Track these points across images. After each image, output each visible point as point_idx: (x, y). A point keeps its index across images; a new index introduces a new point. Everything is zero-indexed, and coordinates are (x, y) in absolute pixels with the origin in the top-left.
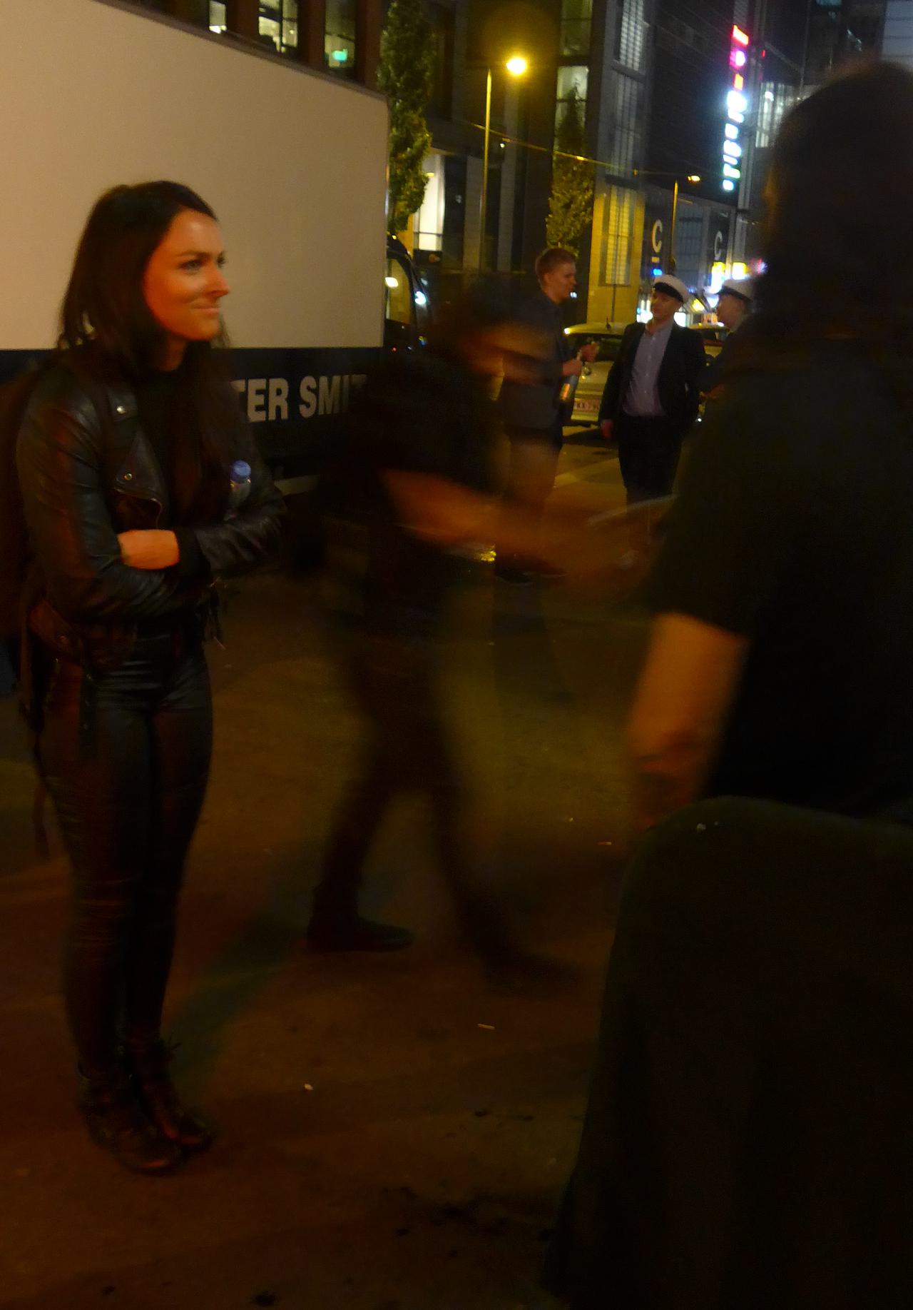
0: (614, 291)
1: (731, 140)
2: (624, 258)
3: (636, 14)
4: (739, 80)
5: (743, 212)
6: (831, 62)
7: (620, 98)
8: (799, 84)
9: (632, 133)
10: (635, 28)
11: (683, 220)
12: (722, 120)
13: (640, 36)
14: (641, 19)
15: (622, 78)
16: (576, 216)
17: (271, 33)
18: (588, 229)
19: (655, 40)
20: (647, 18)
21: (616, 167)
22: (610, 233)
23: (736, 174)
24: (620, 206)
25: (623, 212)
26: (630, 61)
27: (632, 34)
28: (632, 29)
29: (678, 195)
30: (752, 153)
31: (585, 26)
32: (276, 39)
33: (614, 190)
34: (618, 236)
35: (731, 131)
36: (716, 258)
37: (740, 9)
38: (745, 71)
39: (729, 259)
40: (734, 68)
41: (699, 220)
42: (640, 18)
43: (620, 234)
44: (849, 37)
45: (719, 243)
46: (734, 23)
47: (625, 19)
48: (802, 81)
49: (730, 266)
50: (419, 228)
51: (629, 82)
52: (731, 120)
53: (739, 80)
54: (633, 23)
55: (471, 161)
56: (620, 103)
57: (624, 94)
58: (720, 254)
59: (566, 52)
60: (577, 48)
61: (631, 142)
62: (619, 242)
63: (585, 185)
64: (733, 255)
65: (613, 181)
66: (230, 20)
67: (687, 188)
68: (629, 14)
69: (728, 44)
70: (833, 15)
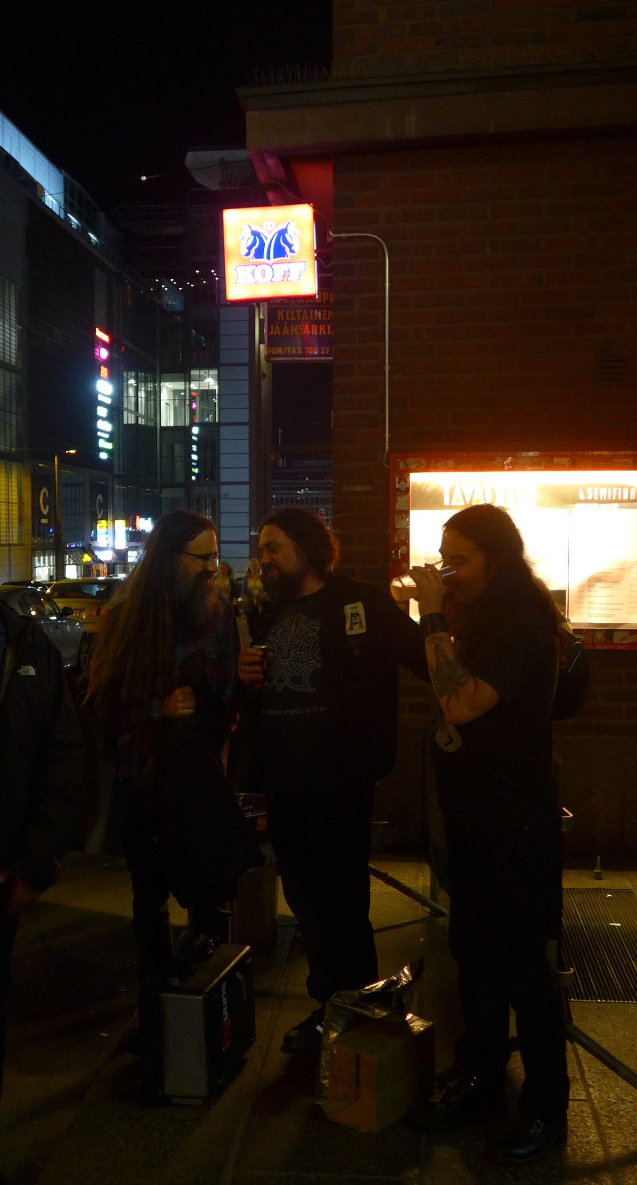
0: (10, 550)
1: (104, 419)
2: (16, 521)
3: (10, 319)
4: (104, 371)
5: (118, 476)
9: (14, 417)
10: (10, 330)
11: (67, 485)
13: (15, 337)
14: (14, 323)
20: (19, 321)
23: (109, 446)
26: (7, 357)
27: (8, 335)
28: (7, 331)
34: (9, 503)
35: (102, 411)
37: (100, 312)
38: (108, 363)
39: (110, 517)
40: (99, 361)
41: (82, 485)
43: (10, 501)
45: (99, 503)
48: (158, 369)
49: (112, 522)
53: (104, 371)
54: (7, 326)
61: (14, 423)
67: (66, 460)
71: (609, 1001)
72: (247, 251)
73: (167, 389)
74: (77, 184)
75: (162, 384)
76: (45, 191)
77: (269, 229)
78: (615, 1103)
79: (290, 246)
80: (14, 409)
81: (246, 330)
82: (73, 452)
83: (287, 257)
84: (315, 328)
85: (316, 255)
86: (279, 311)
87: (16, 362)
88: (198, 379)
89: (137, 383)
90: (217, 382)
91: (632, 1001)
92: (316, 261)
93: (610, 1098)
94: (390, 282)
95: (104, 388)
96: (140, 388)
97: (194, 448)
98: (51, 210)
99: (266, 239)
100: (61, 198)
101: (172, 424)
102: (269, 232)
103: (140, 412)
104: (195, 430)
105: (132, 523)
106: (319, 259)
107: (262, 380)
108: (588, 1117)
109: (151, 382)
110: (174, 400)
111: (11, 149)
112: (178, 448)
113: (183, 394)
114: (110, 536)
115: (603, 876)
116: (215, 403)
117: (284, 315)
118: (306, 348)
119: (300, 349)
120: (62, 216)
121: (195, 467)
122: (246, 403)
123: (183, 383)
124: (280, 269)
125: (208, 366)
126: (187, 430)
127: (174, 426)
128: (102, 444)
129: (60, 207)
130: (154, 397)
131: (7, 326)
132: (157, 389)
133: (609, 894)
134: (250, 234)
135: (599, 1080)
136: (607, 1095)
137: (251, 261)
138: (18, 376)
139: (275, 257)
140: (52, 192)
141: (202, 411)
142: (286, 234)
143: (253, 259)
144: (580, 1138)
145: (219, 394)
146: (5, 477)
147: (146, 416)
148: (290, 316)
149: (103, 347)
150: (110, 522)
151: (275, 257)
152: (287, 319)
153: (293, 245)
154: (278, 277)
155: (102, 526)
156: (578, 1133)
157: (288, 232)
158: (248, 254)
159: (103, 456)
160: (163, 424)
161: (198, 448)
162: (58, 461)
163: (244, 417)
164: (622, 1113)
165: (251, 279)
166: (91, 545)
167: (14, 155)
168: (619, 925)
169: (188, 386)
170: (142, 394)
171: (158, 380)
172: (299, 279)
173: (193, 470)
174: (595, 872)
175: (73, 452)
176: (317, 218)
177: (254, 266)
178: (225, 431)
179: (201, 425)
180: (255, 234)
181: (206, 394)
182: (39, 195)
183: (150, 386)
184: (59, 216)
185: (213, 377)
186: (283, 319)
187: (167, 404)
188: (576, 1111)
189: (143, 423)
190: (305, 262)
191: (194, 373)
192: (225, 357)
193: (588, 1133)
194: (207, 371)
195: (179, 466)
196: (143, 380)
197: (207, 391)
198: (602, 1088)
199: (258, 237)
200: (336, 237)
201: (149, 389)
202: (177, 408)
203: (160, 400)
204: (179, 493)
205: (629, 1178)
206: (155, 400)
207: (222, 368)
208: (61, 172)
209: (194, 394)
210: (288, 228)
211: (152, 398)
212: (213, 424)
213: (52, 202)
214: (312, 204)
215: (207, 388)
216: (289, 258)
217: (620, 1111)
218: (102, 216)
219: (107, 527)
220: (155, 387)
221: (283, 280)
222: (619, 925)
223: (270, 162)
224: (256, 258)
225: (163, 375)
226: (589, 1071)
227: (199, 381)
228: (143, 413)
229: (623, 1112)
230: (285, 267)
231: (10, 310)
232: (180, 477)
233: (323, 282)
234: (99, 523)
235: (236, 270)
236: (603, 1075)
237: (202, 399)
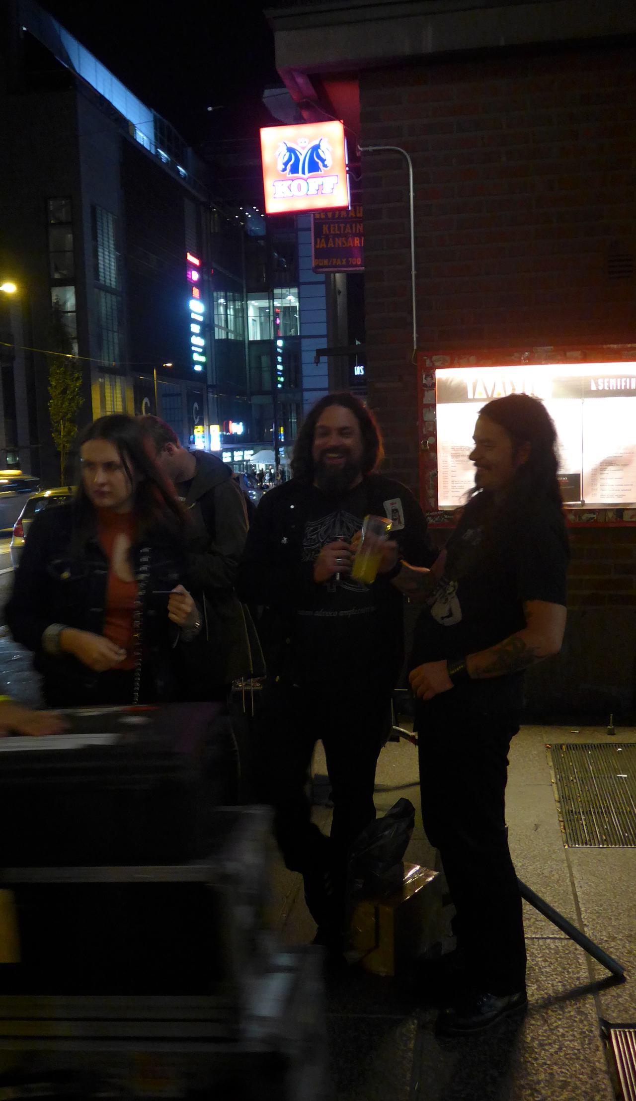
1: (197, 335)
3: (109, 246)
4: (196, 292)
5: (212, 386)
7: (103, 308)
10: (109, 256)
11: (165, 395)
14: (113, 250)
15: (102, 294)
16: (72, 400)
19: (126, 266)
20: (117, 248)
21: (106, 363)
22: (107, 410)
23: (203, 359)
24: (113, 387)
26: (108, 281)
27: (107, 261)
28: (107, 257)
29: (157, 377)
30: (213, 341)
33: (107, 376)
35: (195, 328)
37: (190, 237)
38: (200, 284)
39: (206, 423)
41: (179, 395)
46: (187, 250)
47: (100, 250)
48: (245, 290)
51: (109, 295)
52: (194, 319)
53: (196, 292)
54: (106, 253)
57: (106, 305)
58: (198, 420)
59: (57, 276)
60: (65, 272)
61: (116, 341)
64: (208, 418)
67: (163, 372)
68: (103, 246)
70: (262, 242)
71: (610, 846)
72: (283, 167)
73: (253, 307)
74: (166, 122)
75: (249, 302)
76: (136, 128)
77: (304, 145)
78: (606, 941)
79: (323, 161)
82: (169, 365)
83: (321, 171)
84: (357, 240)
85: (347, 169)
86: (324, 225)
87: (116, 286)
88: (280, 297)
89: (226, 301)
90: (297, 299)
91: (631, 845)
92: (348, 175)
93: (602, 936)
94: (414, 191)
95: (196, 307)
96: (229, 306)
97: (279, 359)
98: (142, 146)
99: (301, 155)
100: (152, 136)
101: (259, 338)
102: (303, 148)
104: (280, 343)
105: (225, 428)
106: (351, 172)
107: (338, 296)
108: (581, 954)
109: (238, 300)
110: (260, 316)
111: (104, 90)
112: (265, 360)
113: (267, 310)
114: (206, 440)
115: (616, 732)
116: (297, 318)
117: (329, 228)
118: (350, 259)
119: (344, 260)
120: (153, 152)
121: (281, 376)
122: (324, 319)
123: (267, 301)
124: (314, 183)
125: (289, 285)
126: (271, 344)
127: (260, 341)
128: (196, 357)
129: (151, 143)
130: (242, 314)
131: (106, 253)
132: (245, 307)
133: (619, 748)
134: (286, 151)
135: (594, 919)
136: (599, 933)
137: (288, 175)
138: (119, 298)
139: (309, 172)
140: (143, 129)
141: (285, 326)
142: (319, 150)
143: (289, 174)
144: (571, 975)
145: (300, 310)
146: (110, 389)
147: (235, 332)
148: (334, 230)
149: (194, 270)
150: (206, 427)
151: (309, 172)
152: (332, 232)
153: (325, 160)
154: (313, 191)
155: (199, 431)
156: (570, 970)
157: (321, 147)
158: (284, 170)
159: (198, 368)
160: (251, 339)
161: (283, 359)
163: (322, 329)
164: (612, 950)
165: (288, 193)
166: (189, 448)
167: (107, 96)
168: (626, 776)
170: (231, 312)
171: (245, 299)
172: (332, 193)
173: (279, 379)
174: (609, 729)
175: (169, 365)
176: (347, 134)
177: (290, 182)
178: (305, 343)
179: (284, 338)
180: (291, 150)
181: (288, 311)
182: (131, 132)
183: (238, 304)
184: (149, 152)
186: (328, 233)
187: (254, 320)
188: (571, 949)
189: (233, 338)
190: (337, 176)
191: (277, 291)
192: (304, 277)
193: (578, 969)
195: (266, 376)
196: (231, 298)
197: (289, 308)
198: (596, 927)
199: (293, 154)
200: (365, 151)
201: (237, 307)
202: (263, 324)
203: (248, 317)
204: (266, 400)
205: (612, 1011)
206: (243, 317)
207: (302, 287)
208: (151, 112)
209: (277, 310)
210: (321, 144)
212: (296, 337)
213: (143, 139)
214: (342, 121)
215: (289, 305)
216: (323, 172)
217: (611, 948)
218: (189, 150)
219: (203, 431)
220: (242, 305)
221: (317, 194)
222: (626, 776)
223: (300, 80)
224: (292, 174)
226: (586, 911)
227: (281, 298)
228: (232, 329)
229: (612, 949)
230: (319, 181)
231: (108, 238)
232: (267, 386)
233: (354, 197)
234: (197, 428)
235: (274, 185)
236: (597, 915)
237: (285, 315)
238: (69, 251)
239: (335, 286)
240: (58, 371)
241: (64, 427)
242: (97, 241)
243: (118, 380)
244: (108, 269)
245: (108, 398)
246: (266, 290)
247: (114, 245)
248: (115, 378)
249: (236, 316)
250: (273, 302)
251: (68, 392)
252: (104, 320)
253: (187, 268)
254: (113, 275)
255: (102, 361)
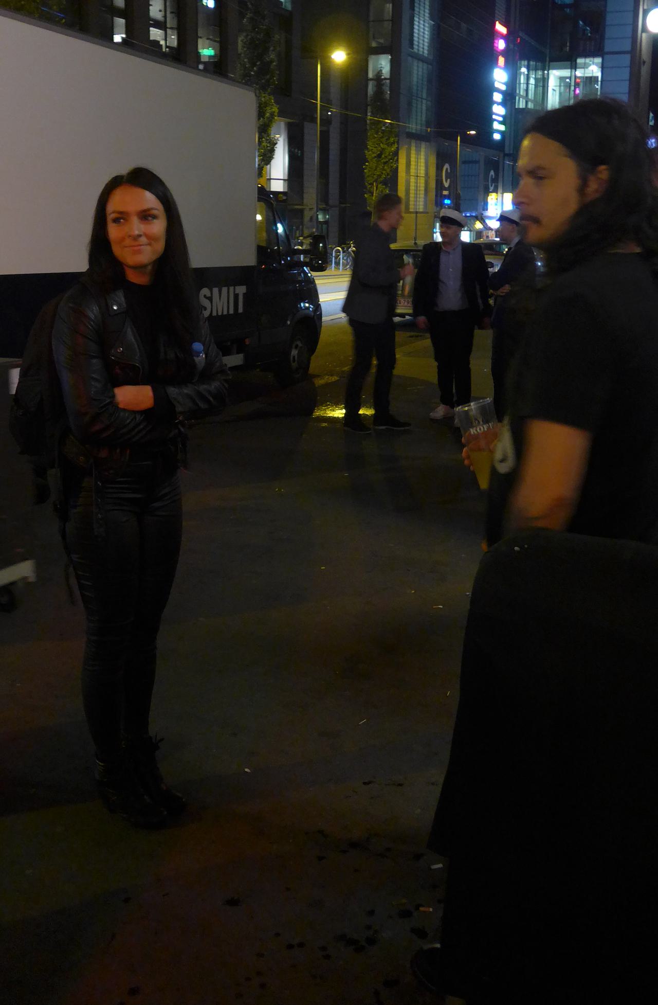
0: (416, 216)
1: (498, 104)
2: (423, 192)
3: (424, 15)
4: (501, 60)
6: (568, 44)
8: (546, 62)
9: (424, 101)
10: (424, 25)
11: (464, 162)
12: (492, 89)
15: (415, 63)
17: (158, 39)
18: (395, 172)
19: (438, 34)
20: (432, 17)
21: (414, 126)
22: (411, 174)
23: (502, 128)
25: (420, 159)
26: (421, 50)
28: (422, 26)
29: (460, 145)
31: (388, 26)
32: (162, 43)
34: (417, 176)
35: (498, 97)
36: (490, 190)
38: (505, 53)
39: (500, 190)
40: (497, 51)
41: (477, 162)
42: (427, 18)
43: (419, 175)
44: (580, 26)
46: (496, 19)
47: (416, 19)
48: (548, 59)
49: (501, 195)
50: (270, 176)
51: (421, 64)
53: (501, 60)
54: (422, 22)
55: (307, 126)
56: (415, 79)
57: (418, 73)
59: (374, 44)
60: (382, 41)
61: (424, 108)
62: (419, 181)
63: (392, 140)
64: (503, 186)
65: (412, 136)
66: (129, 30)
67: (466, 140)
68: (419, 15)
69: (494, 34)
70: (568, 10)
73: (555, 75)
75: (550, 71)
80: (424, 96)
81: (630, 21)
82: (473, 132)
87: (428, 54)
89: (528, 71)
90: (600, 69)
95: (500, 76)
103: (530, 97)
107: (642, 66)
109: (541, 70)
110: (560, 86)
113: (568, 80)
123: (569, 70)
125: (593, 55)
128: (496, 126)
130: (543, 83)
131: (422, 22)
132: (546, 76)
138: (430, 67)
145: (601, 82)
147: (535, 101)
149: (501, 38)
150: (500, 195)
155: (492, 198)
159: (497, 137)
162: (460, 142)
166: (483, 214)
169: (573, 73)
170: (532, 81)
171: (547, 68)
175: (473, 132)
181: (591, 80)
183: (540, 73)
185: (597, 65)
187: (553, 90)
191: (580, 61)
192: (609, 46)
194: (592, 59)
197: (591, 78)
201: (539, 77)
203: (548, 86)
207: (607, 57)
211: (541, 85)
215: (591, 75)
219: (497, 199)
225: (551, 63)
227: (584, 68)
228: (533, 99)
231: (424, 7)
238: (388, 20)
239: (640, 54)
240: (376, 136)
241: (377, 189)
242: (414, 10)
243: (423, 145)
244: (421, 38)
245: (413, 163)
246: (569, 59)
247: (429, 10)
248: (421, 144)
249: (536, 86)
250: (575, 71)
251: (383, 156)
252: (415, 88)
253: (495, 37)
254: (426, 44)
255: (410, 126)
